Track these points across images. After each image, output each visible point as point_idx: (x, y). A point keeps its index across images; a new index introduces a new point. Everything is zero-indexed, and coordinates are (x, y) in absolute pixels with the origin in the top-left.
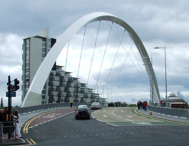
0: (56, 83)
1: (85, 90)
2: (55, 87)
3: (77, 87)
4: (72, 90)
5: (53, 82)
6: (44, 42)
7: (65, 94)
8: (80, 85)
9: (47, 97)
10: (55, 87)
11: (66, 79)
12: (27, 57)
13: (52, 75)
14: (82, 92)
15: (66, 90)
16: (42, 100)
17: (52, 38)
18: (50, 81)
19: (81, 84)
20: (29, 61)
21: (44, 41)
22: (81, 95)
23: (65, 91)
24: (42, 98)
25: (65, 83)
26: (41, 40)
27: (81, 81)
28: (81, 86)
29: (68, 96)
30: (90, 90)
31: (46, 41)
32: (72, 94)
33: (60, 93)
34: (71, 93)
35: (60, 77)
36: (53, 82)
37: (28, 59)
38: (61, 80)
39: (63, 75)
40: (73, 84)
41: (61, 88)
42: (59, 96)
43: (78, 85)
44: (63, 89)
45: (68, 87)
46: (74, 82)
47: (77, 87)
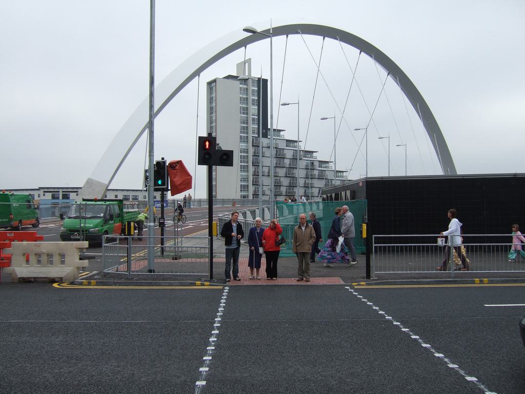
0: (268, 162)
4: (300, 173)
6: (245, 86)
7: (285, 182)
8: (316, 164)
9: (251, 189)
11: (289, 154)
15: (290, 175)
16: (241, 193)
18: (255, 157)
19: (320, 161)
23: (286, 177)
24: (241, 190)
25: (287, 162)
26: (237, 84)
27: (319, 156)
29: (292, 186)
31: (247, 85)
37: (214, 118)
38: (280, 155)
39: (282, 145)
40: (302, 164)
41: (278, 170)
44: (281, 172)
45: (293, 168)
46: (304, 159)
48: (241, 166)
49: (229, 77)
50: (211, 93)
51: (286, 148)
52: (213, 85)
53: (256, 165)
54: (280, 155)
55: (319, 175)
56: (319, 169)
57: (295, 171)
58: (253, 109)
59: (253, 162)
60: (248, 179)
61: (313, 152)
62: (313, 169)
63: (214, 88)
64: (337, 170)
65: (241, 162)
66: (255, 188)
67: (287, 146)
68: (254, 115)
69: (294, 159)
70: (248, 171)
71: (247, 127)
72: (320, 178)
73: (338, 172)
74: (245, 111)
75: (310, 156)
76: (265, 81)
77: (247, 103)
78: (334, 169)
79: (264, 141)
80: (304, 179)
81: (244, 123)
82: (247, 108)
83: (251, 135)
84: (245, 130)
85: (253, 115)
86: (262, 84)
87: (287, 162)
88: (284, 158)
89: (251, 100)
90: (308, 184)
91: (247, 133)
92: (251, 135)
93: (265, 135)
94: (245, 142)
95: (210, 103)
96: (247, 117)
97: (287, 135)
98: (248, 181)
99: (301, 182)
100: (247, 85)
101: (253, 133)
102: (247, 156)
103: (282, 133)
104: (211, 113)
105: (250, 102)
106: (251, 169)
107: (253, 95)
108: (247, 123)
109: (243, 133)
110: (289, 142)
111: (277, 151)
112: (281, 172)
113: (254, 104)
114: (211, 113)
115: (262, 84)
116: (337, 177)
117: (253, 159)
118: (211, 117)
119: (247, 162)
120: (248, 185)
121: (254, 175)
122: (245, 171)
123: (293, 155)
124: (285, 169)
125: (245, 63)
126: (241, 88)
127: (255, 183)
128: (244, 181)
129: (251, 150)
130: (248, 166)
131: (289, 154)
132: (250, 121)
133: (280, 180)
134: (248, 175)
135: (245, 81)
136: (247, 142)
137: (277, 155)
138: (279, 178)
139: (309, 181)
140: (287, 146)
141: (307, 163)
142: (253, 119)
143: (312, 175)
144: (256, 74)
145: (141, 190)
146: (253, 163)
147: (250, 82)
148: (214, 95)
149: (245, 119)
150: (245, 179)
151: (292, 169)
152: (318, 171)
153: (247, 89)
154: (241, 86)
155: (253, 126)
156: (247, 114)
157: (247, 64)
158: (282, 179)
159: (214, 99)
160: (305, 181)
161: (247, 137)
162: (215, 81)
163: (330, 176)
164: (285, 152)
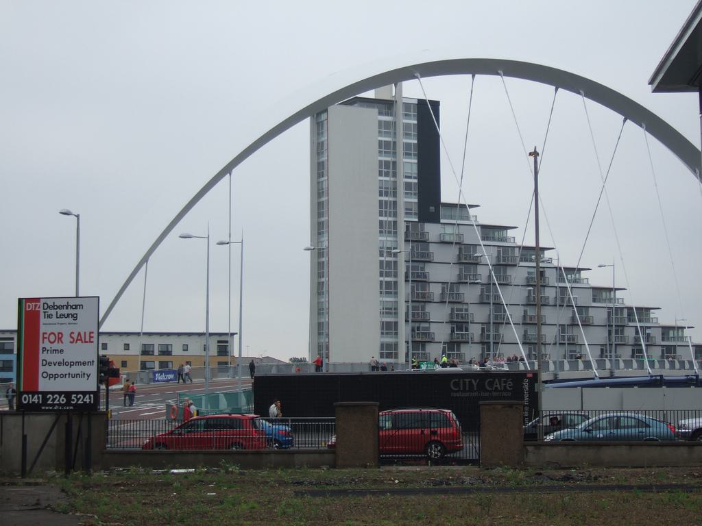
0: (442, 272)
2: (435, 290)
4: (512, 298)
5: (429, 269)
7: (479, 314)
8: (551, 277)
13: (425, 242)
14: (563, 301)
17: (419, 100)
23: (481, 303)
33: (458, 310)
35: (458, 246)
36: (429, 269)
38: (467, 260)
41: (463, 290)
42: (459, 324)
50: (318, 134)
58: (409, 165)
68: (410, 177)
70: (396, 293)
71: (395, 203)
74: (388, 168)
77: (395, 153)
79: (432, 231)
80: (522, 308)
83: (402, 219)
84: (388, 208)
85: (407, 177)
88: (477, 264)
91: (395, 215)
92: (402, 219)
93: (435, 219)
94: (390, 232)
101: (407, 213)
102: (396, 263)
105: (401, 150)
106: (404, 290)
108: (395, 195)
113: (410, 154)
119: (396, 276)
122: (391, 293)
128: (386, 313)
129: (404, 250)
130: (396, 283)
131: (487, 254)
132: (401, 190)
133: (467, 310)
136: (395, 233)
138: (465, 307)
141: (529, 273)
142: (408, 186)
149: (390, 186)
152: (554, 289)
156: (395, 175)
160: (525, 312)
161: (395, 223)
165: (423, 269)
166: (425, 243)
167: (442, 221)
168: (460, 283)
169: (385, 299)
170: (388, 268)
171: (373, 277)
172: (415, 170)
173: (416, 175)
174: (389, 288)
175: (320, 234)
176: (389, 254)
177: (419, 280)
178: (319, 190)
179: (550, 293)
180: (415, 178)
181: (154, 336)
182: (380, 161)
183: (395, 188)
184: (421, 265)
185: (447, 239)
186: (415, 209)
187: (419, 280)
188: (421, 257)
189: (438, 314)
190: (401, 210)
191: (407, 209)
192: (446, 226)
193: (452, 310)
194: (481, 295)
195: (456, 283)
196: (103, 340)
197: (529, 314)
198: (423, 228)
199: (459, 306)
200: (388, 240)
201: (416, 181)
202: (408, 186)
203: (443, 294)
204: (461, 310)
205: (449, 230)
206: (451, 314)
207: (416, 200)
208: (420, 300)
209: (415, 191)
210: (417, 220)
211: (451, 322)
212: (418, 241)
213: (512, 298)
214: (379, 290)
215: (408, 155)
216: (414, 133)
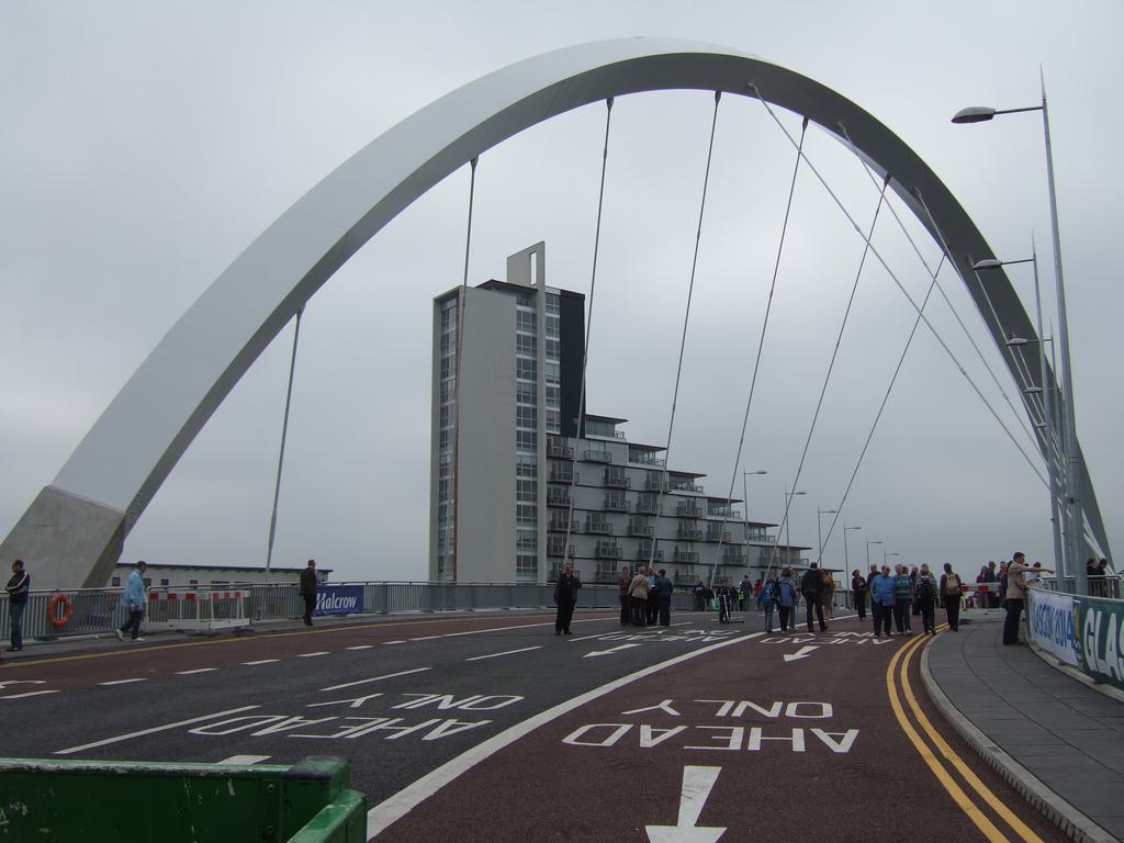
0: (586, 497)
1: (728, 528)
3: (687, 515)
4: (663, 528)
5: (573, 492)
7: (629, 550)
8: (703, 506)
10: (581, 519)
11: (637, 480)
12: (447, 379)
18: (552, 486)
19: (711, 500)
20: (456, 397)
21: (527, 305)
22: (710, 555)
23: (631, 537)
24: (519, 570)
25: (632, 499)
26: (511, 303)
27: (710, 487)
28: (710, 513)
30: (756, 531)
31: (534, 306)
32: (668, 550)
33: (604, 544)
34: (662, 546)
35: (604, 467)
37: (451, 386)
38: (614, 484)
39: (620, 457)
40: (668, 505)
41: (610, 519)
43: (694, 507)
44: (619, 525)
45: (647, 515)
46: (674, 492)
47: (687, 515)
48: (519, 507)
49: (491, 285)
51: (630, 464)
52: (450, 304)
53: (562, 507)
54: (614, 484)
55: (709, 532)
56: (709, 518)
57: (652, 522)
58: (550, 366)
59: (548, 497)
60: (535, 540)
61: (692, 476)
62: (696, 519)
63: (452, 313)
64: (750, 520)
65: (519, 498)
66: (554, 565)
67: (630, 460)
68: (552, 382)
69: (651, 492)
71: (535, 410)
72: (711, 541)
73: (753, 525)
74: (529, 369)
75: (684, 485)
76: (582, 297)
77: (535, 352)
78: (744, 520)
79: (577, 447)
80: (673, 544)
81: (526, 400)
82: (535, 363)
83: (543, 431)
84: (528, 416)
85: (548, 381)
86: (572, 306)
87: (632, 499)
88: (624, 490)
89: (544, 343)
90: (683, 556)
92: (543, 431)
94: (529, 446)
95: (443, 349)
96: (535, 386)
97: (631, 433)
98: (535, 546)
99: (668, 550)
100: (534, 306)
101: (548, 424)
102: (535, 483)
103: (618, 427)
104: (444, 374)
105: (542, 348)
106: (544, 516)
107: (549, 331)
108: (535, 401)
109: (524, 426)
110: (636, 449)
111: (607, 471)
112: (619, 525)
113: (552, 354)
114: (444, 374)
115: (572, 306)
116: (750, 538)
117: (549, 490)
118: (442, 384)
119: (535, 499)
120: (535, 558)
121: (552, 532)
122: (529, 520)
123: (647, 483)
124: (627, 517)
125: (529, 252)
126: (519, 312)
127: (554, 553)
129: (544, 469)
130: (535, 508)
131: (637, 480)
132: (542, 395)
133: (614, 544)
134: (536, 532)
135: (527, 294)
136: (535, 447)
137: (606, 482)
138: (612, 540)
139: (683, 548)
140: (630, 460)
142: (550, 392)
143: (692, 533)
144: (560, 277)
145: (261, 570)
146: (548, 502)
147: (542, 300)
148: (452, 329)
150: (529, 542)
151: (644, 518)
153: (534, 316)
154: (520, 308)
155: (549, 409)
156: (535, 377)
157: (534, 256)
158: (620, 543)
159: (452, 339)
160: (676, 548)
162: (454, 294)
163: (736, 535)
164: (628, 474)
165: (566, 492)
166: (569, 460)
167: (587, 436)
168: (605, 512)
169: (523, 528)
170: (526, 490)
171: (510, 502)
172: (558, 374)
173: (558, 380)
174: (527, 514)
175: (443, 446)
176: (527, 473)
177: (559, 505)
178: (442, 393)
179: (702, 527)
180: (557, 383)
181: (201, 571)
182: (519, 359)
183: (535, 393)
184: (563, 488)
185: (594, 457)
186: (557, 421)
187: (559, 505)
188: (561, 481)
189: (583, 547)
190: (542, 420)
191: (548, 419)
192: (592, 443)
193: (598, 543)
194: (630, 528)
195: (605, 512)
196: (116, 573)
197: (680, 550)
198: (566, 443)
199: (606, 540)
200: (525, 455)
201: (558, 386)
202: (550, 392)
203: (587, 525)
204: (607, 544)
205: (594, 447)
206: (597, 549)
207: (558, 410)
208: (557, 530)
209: (557, 398)
210: (558, 433)
211: (597, 558)
212: (559, 458)
213: (663, 528)
214: (516, 517)
215: (549, 354)
216: (556, 329)
